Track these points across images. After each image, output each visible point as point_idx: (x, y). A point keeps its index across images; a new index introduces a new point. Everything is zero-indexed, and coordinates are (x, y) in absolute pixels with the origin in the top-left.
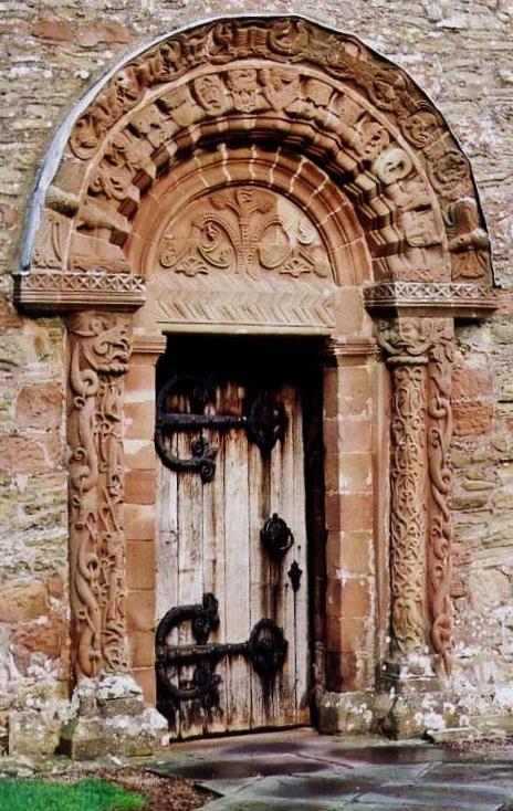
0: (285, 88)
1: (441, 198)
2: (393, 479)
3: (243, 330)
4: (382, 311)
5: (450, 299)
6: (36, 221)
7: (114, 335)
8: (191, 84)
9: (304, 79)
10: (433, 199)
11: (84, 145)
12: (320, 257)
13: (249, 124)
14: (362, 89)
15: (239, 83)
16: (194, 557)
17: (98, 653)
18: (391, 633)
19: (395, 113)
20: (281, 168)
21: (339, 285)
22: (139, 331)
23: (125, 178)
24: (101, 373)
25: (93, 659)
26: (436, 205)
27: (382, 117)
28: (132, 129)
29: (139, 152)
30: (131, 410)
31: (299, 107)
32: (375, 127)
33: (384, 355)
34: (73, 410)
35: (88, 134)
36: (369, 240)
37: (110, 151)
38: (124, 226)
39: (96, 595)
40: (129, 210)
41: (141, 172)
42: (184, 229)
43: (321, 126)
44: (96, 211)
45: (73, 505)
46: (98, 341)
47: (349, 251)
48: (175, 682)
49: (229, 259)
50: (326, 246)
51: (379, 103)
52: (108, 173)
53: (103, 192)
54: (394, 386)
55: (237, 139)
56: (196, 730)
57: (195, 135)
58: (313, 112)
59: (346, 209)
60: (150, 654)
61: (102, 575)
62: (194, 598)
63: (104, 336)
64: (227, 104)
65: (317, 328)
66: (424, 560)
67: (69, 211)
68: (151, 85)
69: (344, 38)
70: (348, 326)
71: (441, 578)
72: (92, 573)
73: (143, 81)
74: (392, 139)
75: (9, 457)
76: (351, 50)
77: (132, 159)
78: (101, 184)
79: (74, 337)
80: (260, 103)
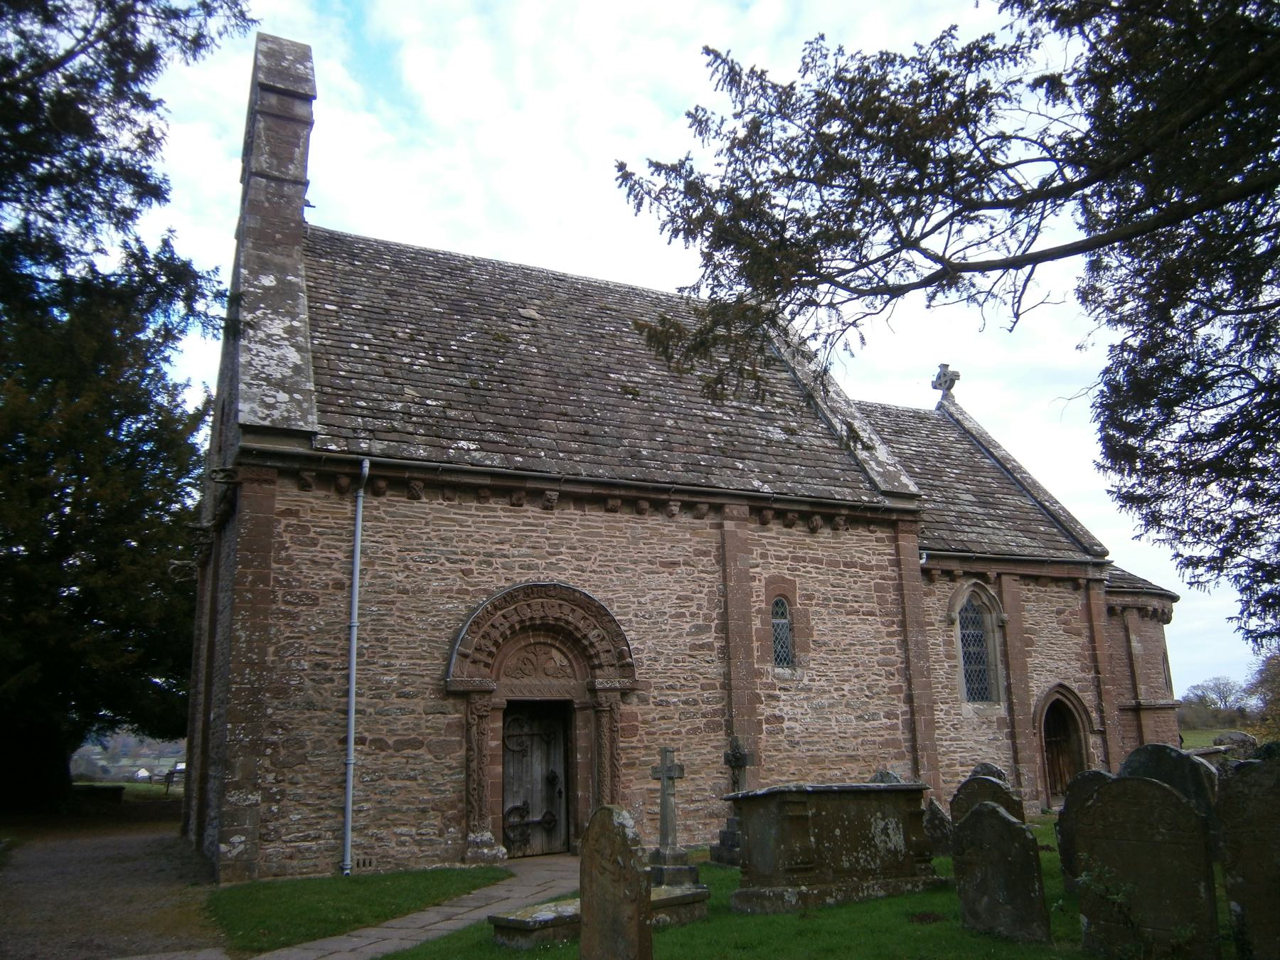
5: (617, 685)
6: (454, 660)
8: (515, 609)
9: (560, 605)
12: (569, 670)
13: (538, 622)
14: (582, 608)
15: (535, 607)
20: (553, 638)
24: (479, 716)
25: (474, 825)
28: (493, 626)
29: (495, 634)
31: (558, 615)
32: (588, 622)
35: (474, 628)
38: (490, 661)
42: (514, 661)
43: (567, 622)
44: (478, 656)
45: (468, 767)
48: (512, 835)
50: (571, 666)
52: (483, 642)
53: (480, 649)
55: (534, 628)
56: (520, 854)
58: (563, 617)
62: (519, 803)
63: (480, 702)
64: (529, 615)
65: (568, 697)
67: (465, 656)
68: (501, 609)
69: (575, 591)
73: (496, 608)
77: (492, 636)
79: (469, 703)
80: (542, 614)
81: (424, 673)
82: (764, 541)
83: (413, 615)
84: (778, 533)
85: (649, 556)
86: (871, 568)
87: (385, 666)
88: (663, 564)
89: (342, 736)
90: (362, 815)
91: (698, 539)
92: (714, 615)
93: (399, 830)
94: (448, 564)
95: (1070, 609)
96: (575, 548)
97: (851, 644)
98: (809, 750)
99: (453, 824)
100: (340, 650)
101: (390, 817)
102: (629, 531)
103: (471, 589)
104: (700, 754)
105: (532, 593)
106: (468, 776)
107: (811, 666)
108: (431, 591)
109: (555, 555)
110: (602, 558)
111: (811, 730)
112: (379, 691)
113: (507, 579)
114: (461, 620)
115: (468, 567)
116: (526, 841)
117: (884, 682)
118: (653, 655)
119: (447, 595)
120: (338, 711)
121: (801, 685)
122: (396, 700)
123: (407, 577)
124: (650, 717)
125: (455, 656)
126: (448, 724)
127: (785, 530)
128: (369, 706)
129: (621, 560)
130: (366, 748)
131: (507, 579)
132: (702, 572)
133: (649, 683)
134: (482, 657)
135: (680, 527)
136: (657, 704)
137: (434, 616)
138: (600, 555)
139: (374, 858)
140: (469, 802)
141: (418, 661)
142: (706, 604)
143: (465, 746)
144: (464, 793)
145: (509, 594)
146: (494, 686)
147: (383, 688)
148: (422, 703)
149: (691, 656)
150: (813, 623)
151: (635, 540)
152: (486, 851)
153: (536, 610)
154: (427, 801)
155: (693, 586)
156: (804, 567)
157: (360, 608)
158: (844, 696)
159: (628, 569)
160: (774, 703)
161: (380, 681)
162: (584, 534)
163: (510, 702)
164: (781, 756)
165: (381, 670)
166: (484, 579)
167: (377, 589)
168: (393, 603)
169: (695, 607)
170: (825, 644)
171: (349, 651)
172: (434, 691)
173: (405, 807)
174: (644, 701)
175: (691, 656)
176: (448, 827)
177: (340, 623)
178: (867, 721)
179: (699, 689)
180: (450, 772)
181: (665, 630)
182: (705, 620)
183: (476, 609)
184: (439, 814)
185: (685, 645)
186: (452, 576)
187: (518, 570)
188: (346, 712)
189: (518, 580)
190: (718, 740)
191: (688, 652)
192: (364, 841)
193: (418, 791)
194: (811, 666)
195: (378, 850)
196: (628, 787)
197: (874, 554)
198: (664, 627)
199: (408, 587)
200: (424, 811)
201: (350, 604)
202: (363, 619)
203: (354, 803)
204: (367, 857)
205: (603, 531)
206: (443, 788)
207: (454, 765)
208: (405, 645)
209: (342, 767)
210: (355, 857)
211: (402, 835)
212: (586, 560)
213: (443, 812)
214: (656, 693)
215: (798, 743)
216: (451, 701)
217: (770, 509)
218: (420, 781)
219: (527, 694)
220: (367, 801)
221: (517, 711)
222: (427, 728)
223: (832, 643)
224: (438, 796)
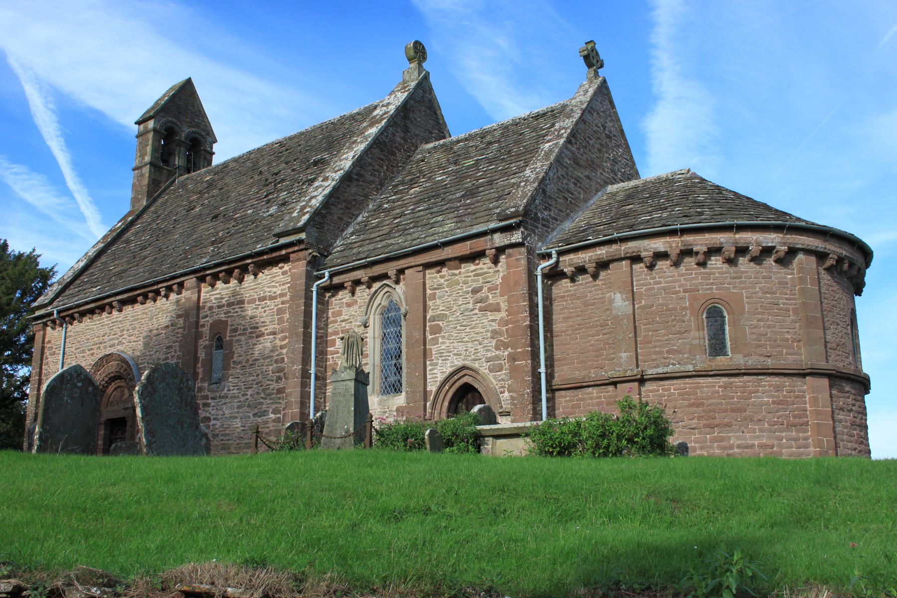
86: (275, 298)
95: (489, 285)
98: (222, 440)
111: (225, 426)
121: (223, 394)
150: (234, 348)
156: (233, 309)
158: (247, 399)
170: (240, 362)
178: (260, 417)
194: (230, 380)
197: (280, 286)
215: (217, 435)
223: (244, 361)
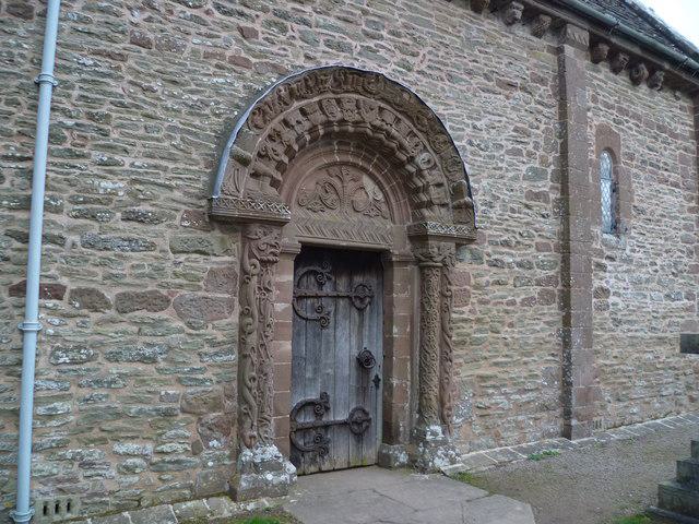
0: (371, 112)
1: (448, 180)
2: (422, 329)
3: (344, 244)
4: (419, 237)
5: (454, 233)
6: (224, 165)
7: (270, 239)
8: (320, 102)
9: (381, 109)
10: (444, 181)
11: (256, 126)
12: (384, 208)
15: (347, 106)
16: (315, 371)
17: (255, 433)
18: (419, 412)
19: (426, 133)
20: (365, 159)
21: (394, 223)
22: (286, 240)
23: (280, 149)
24: (261, 261)
26: (446, 184)
27: (420, 134)
28: (286, 123)
29: (289, 136)
30: (279, 286)
33: (418, 262)
34: (244, 283)
35: (259, 120)
36: (410, 200)
37: (272, 133)
38: (279, 177)
39: (255, 398)
40: (280, 167)
41: (289, 146)
42: (312, 185)
43: (389, 136)
44: (262, 166)
45: (242, 343)
46: (260, 242)
47: (399, 205)
48: (301, 443)
49: (337, 205)
50: (387, 201)
51: (419, 127)
52: (270, 145)
53: (267, 156)
54: (424, 279)
56: (313, 469)
57: (321, 132)
58: (385, 127)
59: (398, 183)
60: (287, 427)
61: (259, 385)
62: (313, 396)
63: (265, 239)
64: (339, 116)
66: (438, 373)
67: (244, 162)
69: (404, 89)
70: (399, 247)
71: (448, 383)
72: (254, 385)
74: (425, 147)
75: (201, 311)
76: (406, 96)
78: (266, 150)
79: (246, 239)
80: (357, 117)
81: (173, 183)
82: (595, 82)
83: (157, 85)
84: (607, 77)
85: (486, 68)
87: (102, 164)
88: (501, 84)
89: (16, 281)
90: (54, 423)
91: (535, 61)
92: (551, 159)
93: (121, 448)
94: (217, 14)
96: (398, 35)
97: (663, 216)
98: (629, 330)
99: (217, 434)
100: (16, 123)
101: (106, 426)
102: (464, 30)
103: (254, 60)
104: (534, 331)
105: (346, 82)
106: (243, 357)
107: (633, 234)
108: (188, 50)
109: (373, 37)
110: (431, 57)
111: (631, 308)
112: (90, 207)
113: (308, 57)
114: (238, 107)
115: (249, 25)
116: (323, 450)
117: (685, 260)
118: (488, 199)
119: (215, 62)
120: (11, 234)
122: (122, 225)
123: (149, 20)
124: (483, 280)
125: (226, 159)
126: (212, 272)
127: (612, 75)
128: (72, 230)
129: (454, 66)
130: (63, 305)
131: (308, 57)
132: (539, 103)
133: (484, 235)
134: (269, 168)
135: (518, 41)
136: (494, 264)
137: (192, 92)
138: (430, 53)
139: (75, 498)
140: (242, 399)
141: (164, 163)
142: (542, 143)
143: (237, 309)
144: (235, 384)
145: (313, 74)
146: (287, 214)
147: (99, 201)
148: (168, 234)
149: (527, 206)
151: (470, 43)
152: (269, 477)
153: (350, 109)
154: (174, 399)
155: (530, 118)
157: (58, 55)
158: (656, 271)
159: (462, 80)
160: (601, 274)
161: (93, 189)
162: (415, 20)
163: (306, 247)
164: (606, 337)
165: (95, 170)
166: (274, 49)
167: (93, 29)
168: (123, 58)
169: (532, 145)
170: (643, 212)
171: (34, 127)
172: (188, 216)
173: (135, 408)
174: (477, 258)
175: (527, 206)
176: (208, 439)
177: (19, 76)
178: (674, 300)
179: (533, 249)
180: (212, 350)
181: (501, 168)
182: (541, 163)
183: (259, 92)
184: (194, 418)
185: (522, 192)
186: (224, 34)
187: (322, 47)
188: (25, 238)
189: (323, 61)
190: (551, 315)
191: (524, 201)
192: (59, 470)
193: (156, 381)
194: (633, 234)
195: (83, 483)
196: (457, 374)
198: (500, 165)
199: (151, 36)
200: (168, 414)
201: (41, 44)
202: (64, 77)
203: (37, 401)
204: (62, 497)
205: (433, 20)
206: (201, 377)
207: (220, 338)
208: (141, 132)
209: (16, 336)
210: (41, 499)
211: (128, 455)
212: (413, 55)
213: (199, 416)
214: (490, 250)
215: (620, 322)
216: (217, 233)
217: (607, 42)
218: (162, 365)
219: (329, 235)
220: (61, 398)
221: (312, 257)
222: (176, 275)
224: (190, 390)
